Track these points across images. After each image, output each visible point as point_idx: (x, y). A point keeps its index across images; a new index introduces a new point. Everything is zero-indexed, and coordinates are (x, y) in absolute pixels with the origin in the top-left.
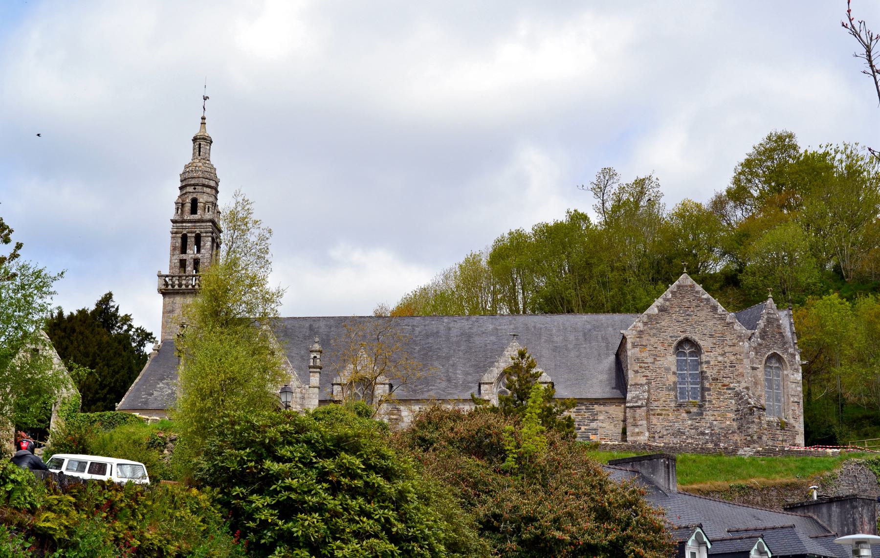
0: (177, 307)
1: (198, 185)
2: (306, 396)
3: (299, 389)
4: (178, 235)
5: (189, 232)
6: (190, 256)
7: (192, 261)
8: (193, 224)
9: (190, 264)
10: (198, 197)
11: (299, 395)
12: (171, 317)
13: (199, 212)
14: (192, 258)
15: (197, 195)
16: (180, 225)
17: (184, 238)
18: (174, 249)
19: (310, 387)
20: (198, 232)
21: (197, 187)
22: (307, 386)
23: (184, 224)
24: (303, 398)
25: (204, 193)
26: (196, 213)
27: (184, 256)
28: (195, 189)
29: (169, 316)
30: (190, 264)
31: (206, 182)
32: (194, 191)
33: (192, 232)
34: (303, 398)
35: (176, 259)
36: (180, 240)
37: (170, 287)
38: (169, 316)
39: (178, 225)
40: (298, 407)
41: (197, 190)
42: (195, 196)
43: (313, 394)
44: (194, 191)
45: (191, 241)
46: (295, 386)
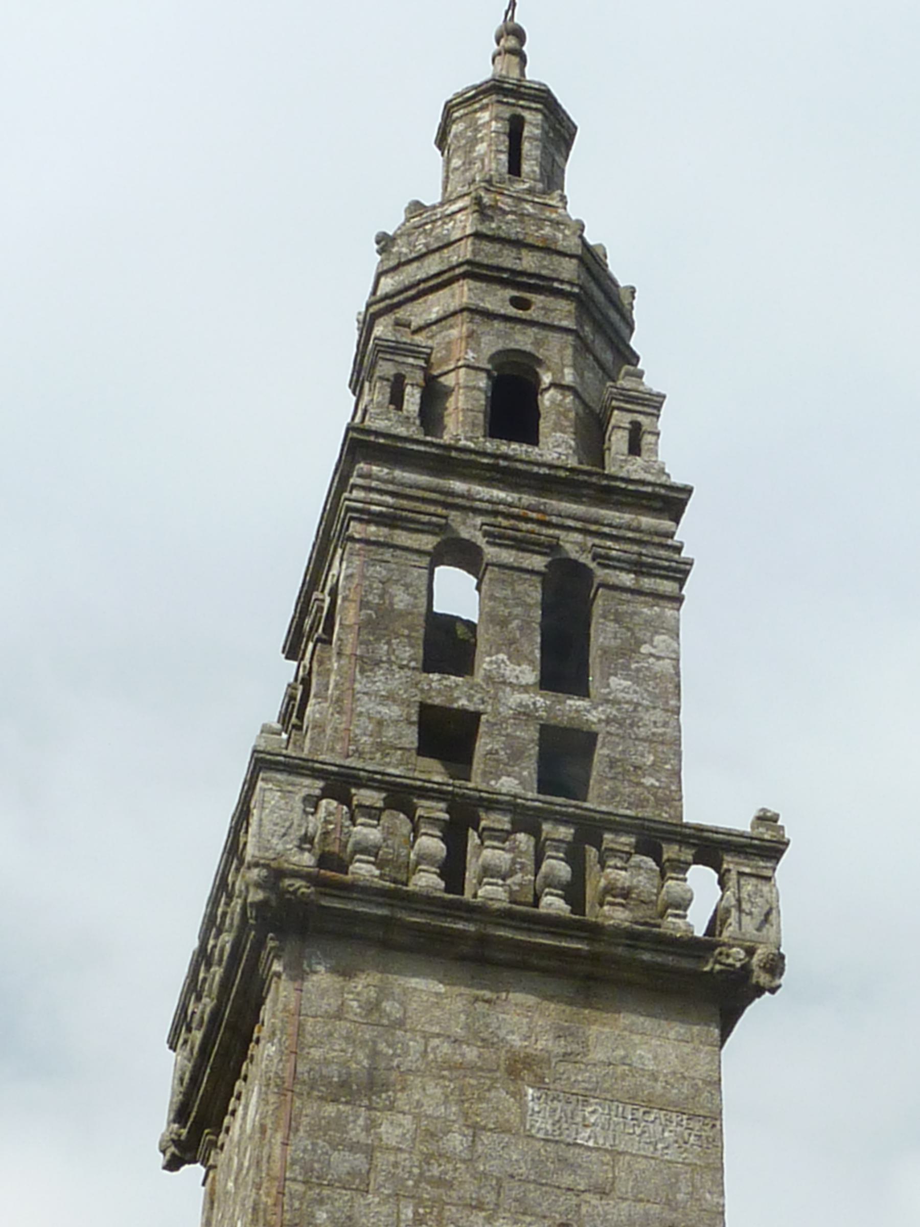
0: (412, 1060)
4: (402, 538)
5: (495, 538)
6: (515, 699)
7: (529, 734)
8: (528, 499)
9: (516, 756)
12: (356, 1133)
14: (524, 714)
15: (537, 343)
16: (424, 479)
21: (538, 299)
23: (458, 486)
26: (532, 437)
28: (519, 303)
29: (339, 1123)
30: (516, 756)
32: (512, 311)
33: (522, 545)
35: (390, 698)
38: (339, 1123)
41: (533, 314)
42: (523, 340)
44: (512, 311)
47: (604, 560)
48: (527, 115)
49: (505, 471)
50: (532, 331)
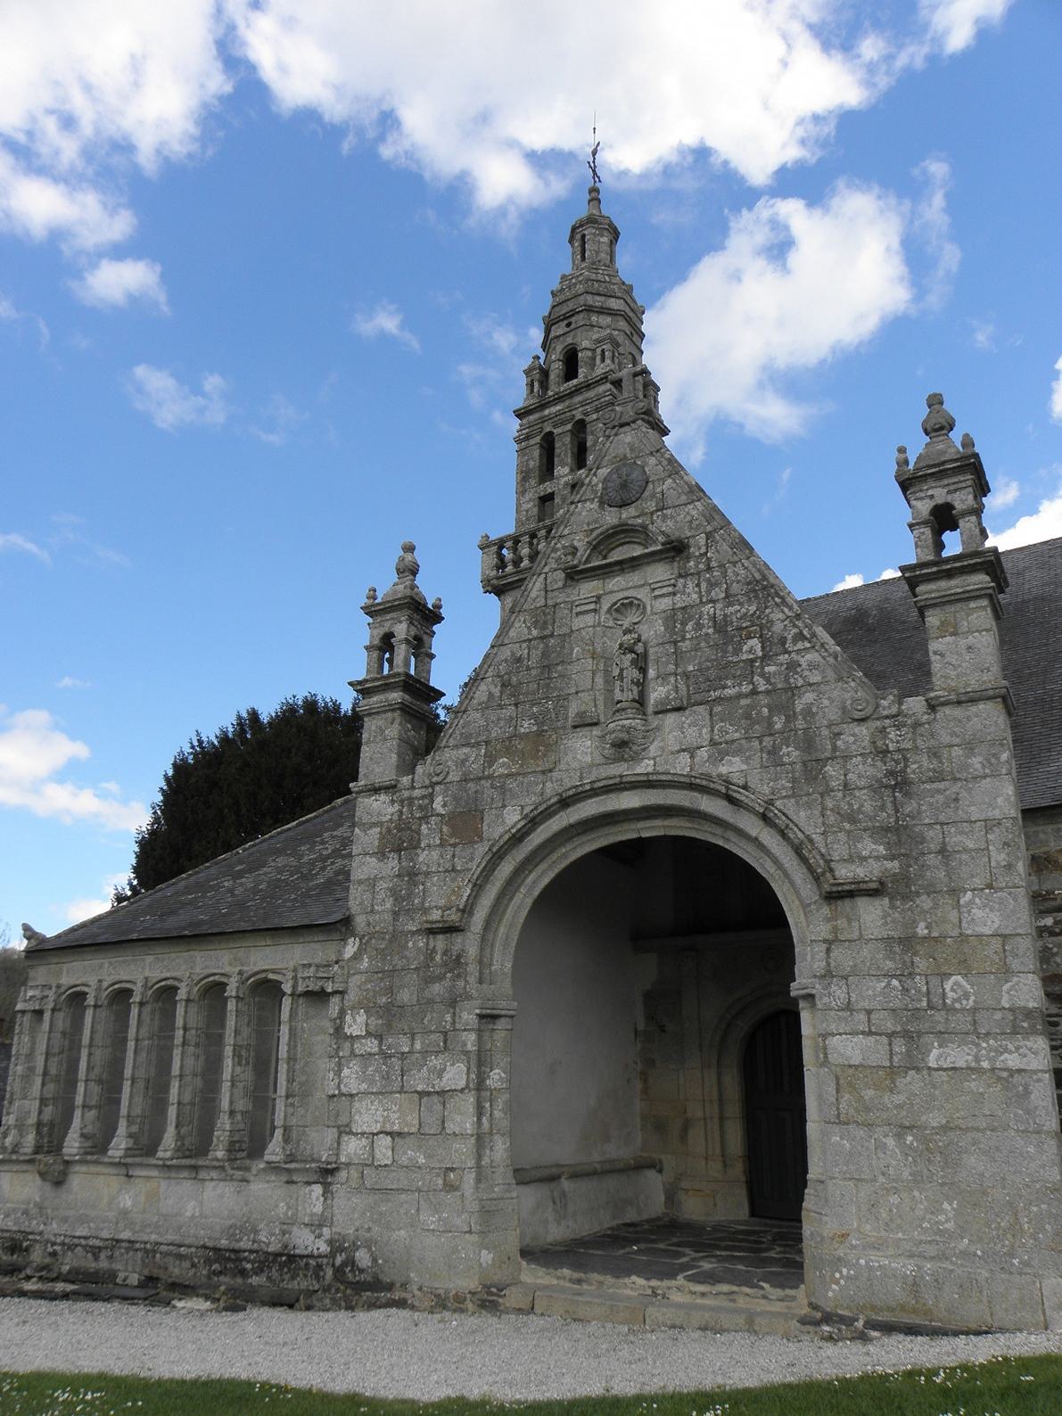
1: (574, 313)
2: (918, 766)
3: (863, 731)
4: (532, 442)
6: (563, 480)
10: (578, 340)
11: (864, 771)
13: (582, 371)
14: (566, 484)
17: (548, 444)
18: (524, 476)
19: (932, 707)
20: (579, 417)
21: (573, 319)
22: (915, 704)
24: (899, 783)
25: (593, 326)
27: (548, 487)
31: (598, 301)
33: (563, 423)
34: (899, 783)
36: (536, 453)
37: (510, 569)
39: (532, 418)
40: (868, 846)
42: (569, 340)
43: (970, 746)
44: (568, 329)
45: (564, 448)
46: (833, 714)
47: (586, 414)
48: (586, 232)
49: (558, 398)
50: (572, 334)
